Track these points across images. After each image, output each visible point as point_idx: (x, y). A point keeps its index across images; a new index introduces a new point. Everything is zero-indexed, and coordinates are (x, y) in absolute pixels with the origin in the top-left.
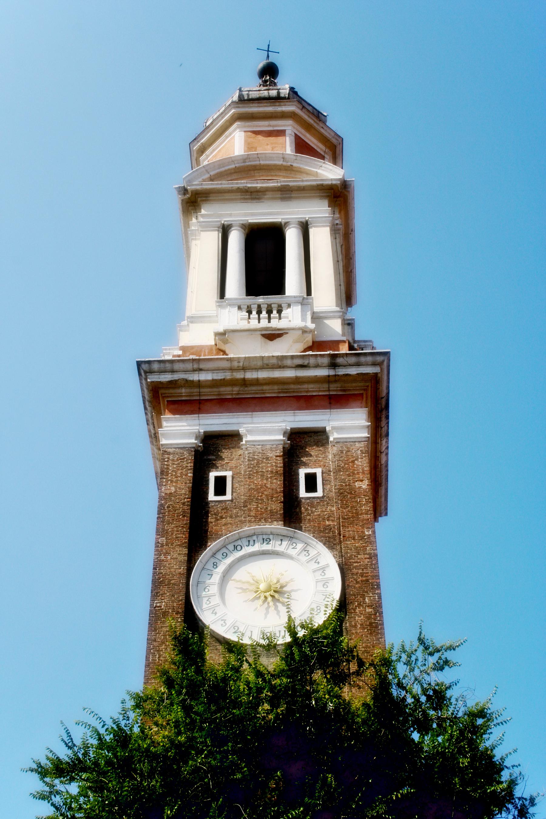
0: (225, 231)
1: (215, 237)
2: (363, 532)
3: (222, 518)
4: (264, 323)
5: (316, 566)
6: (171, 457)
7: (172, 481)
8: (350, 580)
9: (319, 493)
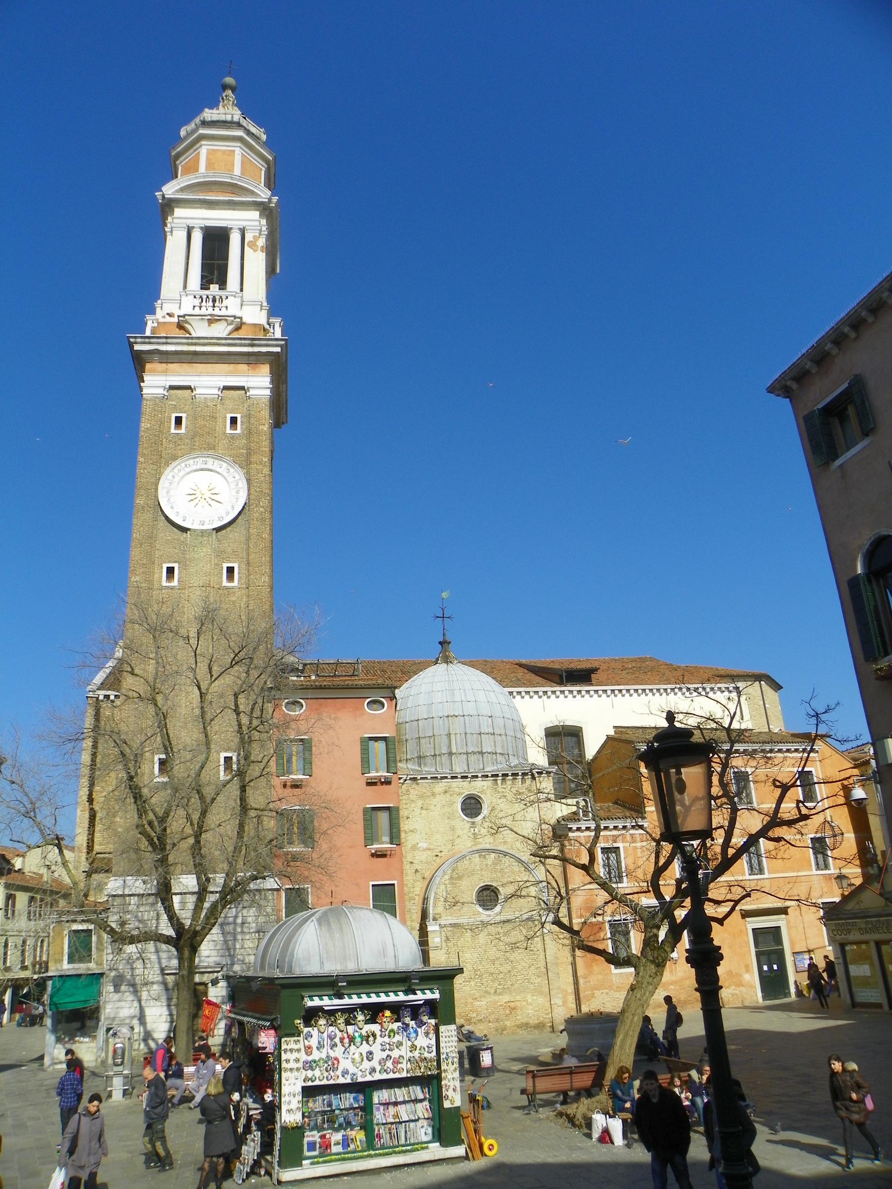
1: (184, 234)
4: (210, 311)
8: (252, 491)
9: (239, 431)
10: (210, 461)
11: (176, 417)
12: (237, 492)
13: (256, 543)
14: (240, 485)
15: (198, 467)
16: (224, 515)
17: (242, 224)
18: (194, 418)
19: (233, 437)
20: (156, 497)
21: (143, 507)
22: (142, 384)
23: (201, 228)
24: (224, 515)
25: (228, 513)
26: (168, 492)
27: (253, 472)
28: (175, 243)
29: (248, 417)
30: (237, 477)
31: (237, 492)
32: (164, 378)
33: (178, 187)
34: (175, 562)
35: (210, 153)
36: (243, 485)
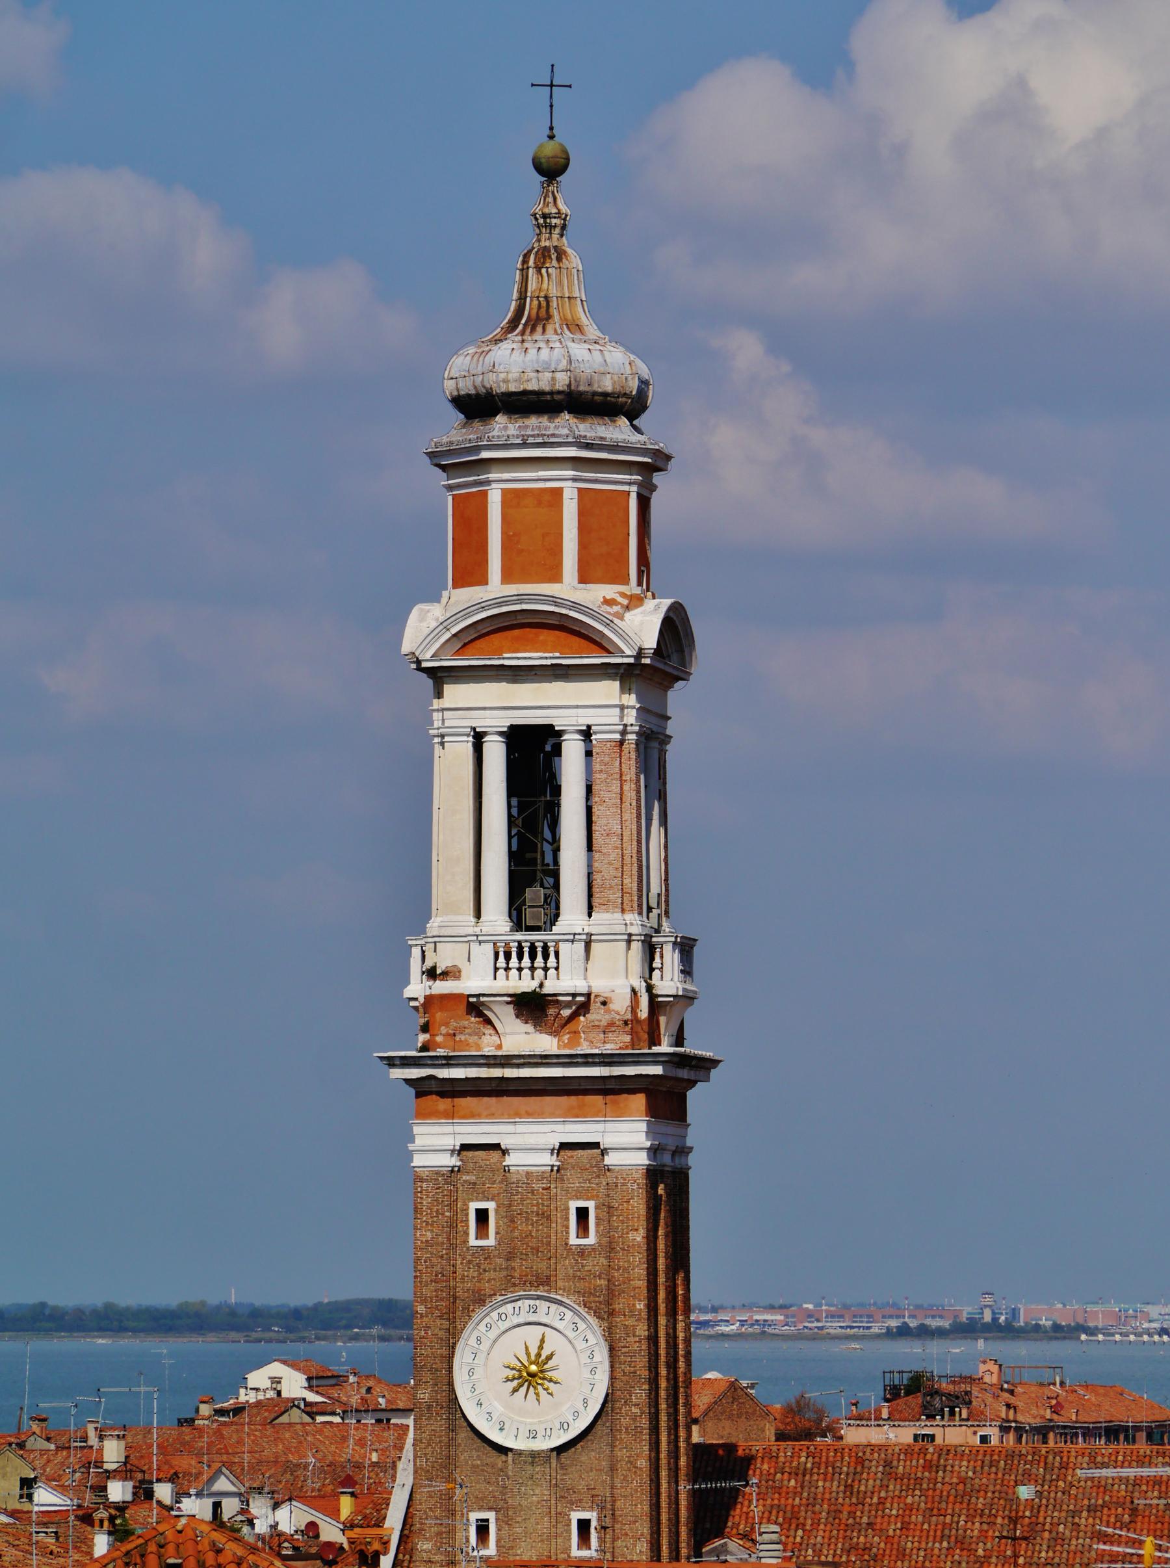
0: (478, 738)
2: (634, 1305)
3: (485, 1270)
5: (584, 1345)
6: (424, 1185)
7: (427, 1223)
10: (543, 1305)
11: (478, 1210)
12: (593, 1371)
13: (625, 1477)
14: (598, 1358)
15: (521, 1320)
16: (570, 1418)
17: (584, 719)
18: (510, 1217)
19: (582, 1251)
20: (451, 1384)
21: (429, 1407)
22: (411, 1147)
23: (501, 734)
24: (570, 1418)
25: (576, 1415)
26: (471, 1372)
27: (619, 1333)
28: (452, 763)
29: (607, 1209)
30: (592, 1340)
31: (593, 1371)
32: (449, 1129)
33: (448, 635)
34: (490, 1509)
35: (511, 499)
36: (602, 1356)
